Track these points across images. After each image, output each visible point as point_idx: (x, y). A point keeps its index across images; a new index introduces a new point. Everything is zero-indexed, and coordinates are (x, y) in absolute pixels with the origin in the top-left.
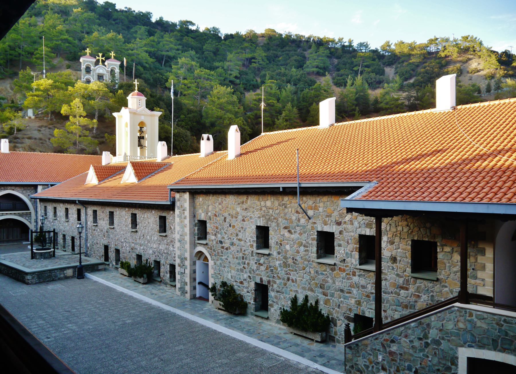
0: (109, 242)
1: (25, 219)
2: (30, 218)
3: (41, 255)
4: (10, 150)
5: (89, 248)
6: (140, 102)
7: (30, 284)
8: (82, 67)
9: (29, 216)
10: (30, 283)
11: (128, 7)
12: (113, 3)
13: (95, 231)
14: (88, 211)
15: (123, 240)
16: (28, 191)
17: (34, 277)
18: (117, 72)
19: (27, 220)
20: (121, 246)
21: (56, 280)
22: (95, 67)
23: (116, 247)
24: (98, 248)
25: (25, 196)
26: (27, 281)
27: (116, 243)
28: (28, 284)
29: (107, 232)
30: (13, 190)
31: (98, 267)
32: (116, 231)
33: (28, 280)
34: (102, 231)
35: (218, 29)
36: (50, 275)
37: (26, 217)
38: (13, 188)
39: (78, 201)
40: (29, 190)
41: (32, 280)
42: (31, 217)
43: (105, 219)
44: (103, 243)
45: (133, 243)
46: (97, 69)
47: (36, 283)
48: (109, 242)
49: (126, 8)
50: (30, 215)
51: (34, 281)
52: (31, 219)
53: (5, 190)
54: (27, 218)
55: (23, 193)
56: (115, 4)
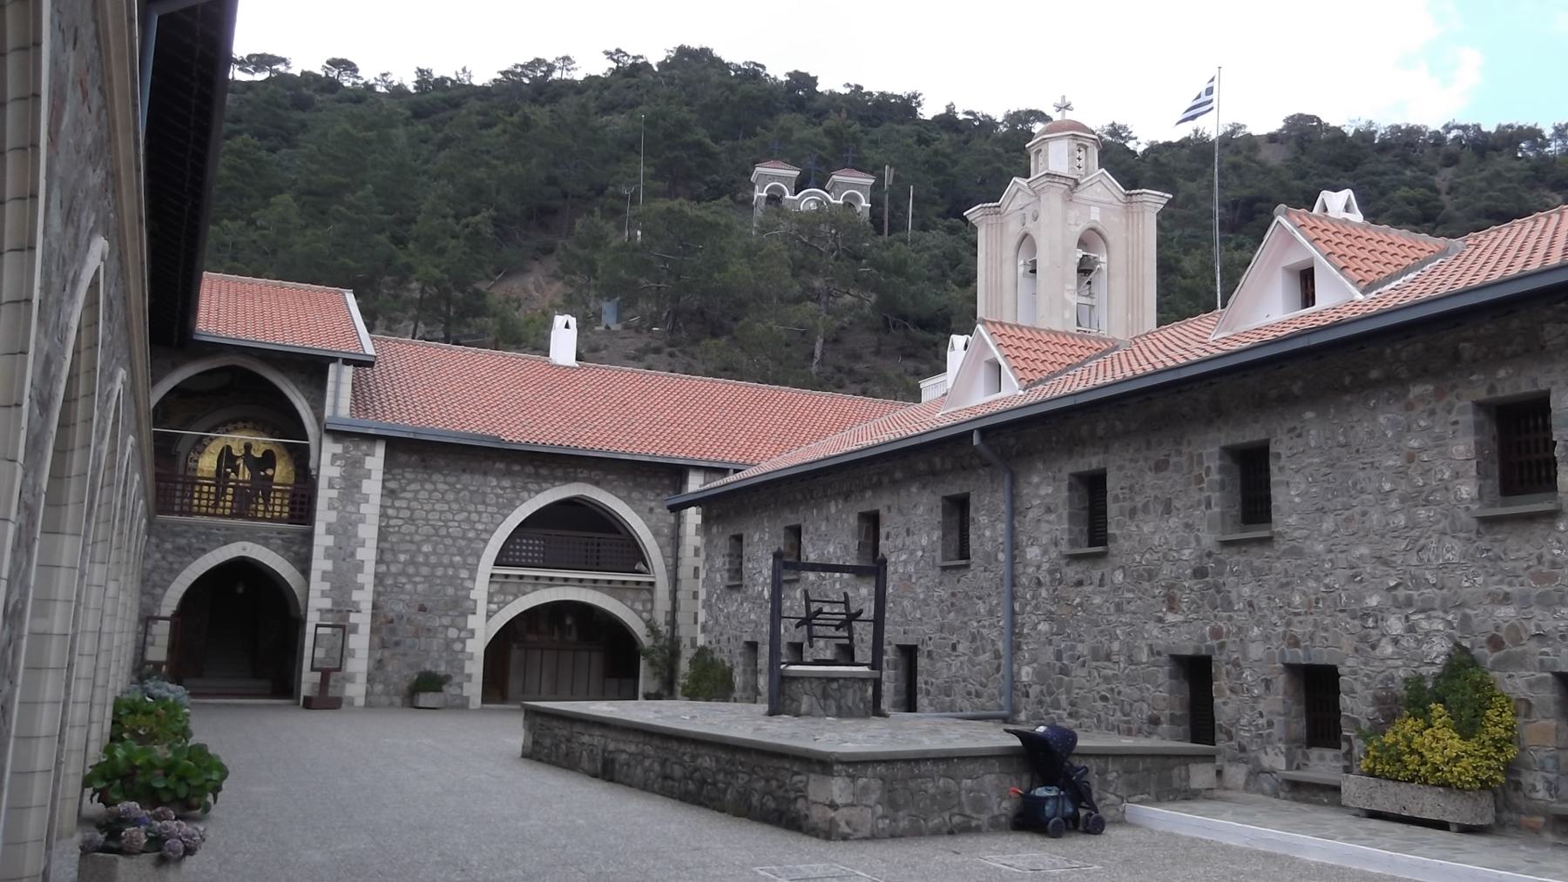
0: (1216, 633)
1: (631, 608)
2: (649, 606)
3: (825, 696)
4: (578, 358)
5: (1034, 691)
6: (1082, 154)
7: (845, 838)
8: (757, 194)
9: (645, 595)
10: (845, 829)
11: (852, 83)
12: (812, 74)
13: (1088, 589)
14: (1026, 491)
15: (1373, 601)
16: (651, 495)
17: (865, 790)
18: (863, 208)
19: (639, 614)
20: (1347, 644)
21: (978, 830)
22: (796, 194)
23: (1300, 657)
24: (1107, 679)
25: (637, 512)
26: (817, 815)
27: (1297, 630)
28: (828, 833)
29: (1200, 573)
30: (597, 484)
31: (1188, 778)
32: (1296, 552)
33: (833, 806)
34: (1151, 575)
35: (1125, 128)
36: (947, 793)
37: (633, 602)
38: (596, 474)
39: (984, 431)
40: (653, 488)
41: (854, 811)
42: (652, 601)
43: (1177, 503)
44: (1161, 644)
45: (1506, 599)
46: (801, 199)
47: (873, 837)
48: (1216, 633)
49: (849, 85)
50: (651, 592)
51: (865, 817)
52: (651, 611)
53: (567, 479)
54: (639, 606)
55: (628, 500)
56: (816, 78)
